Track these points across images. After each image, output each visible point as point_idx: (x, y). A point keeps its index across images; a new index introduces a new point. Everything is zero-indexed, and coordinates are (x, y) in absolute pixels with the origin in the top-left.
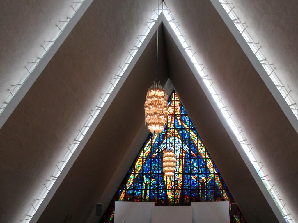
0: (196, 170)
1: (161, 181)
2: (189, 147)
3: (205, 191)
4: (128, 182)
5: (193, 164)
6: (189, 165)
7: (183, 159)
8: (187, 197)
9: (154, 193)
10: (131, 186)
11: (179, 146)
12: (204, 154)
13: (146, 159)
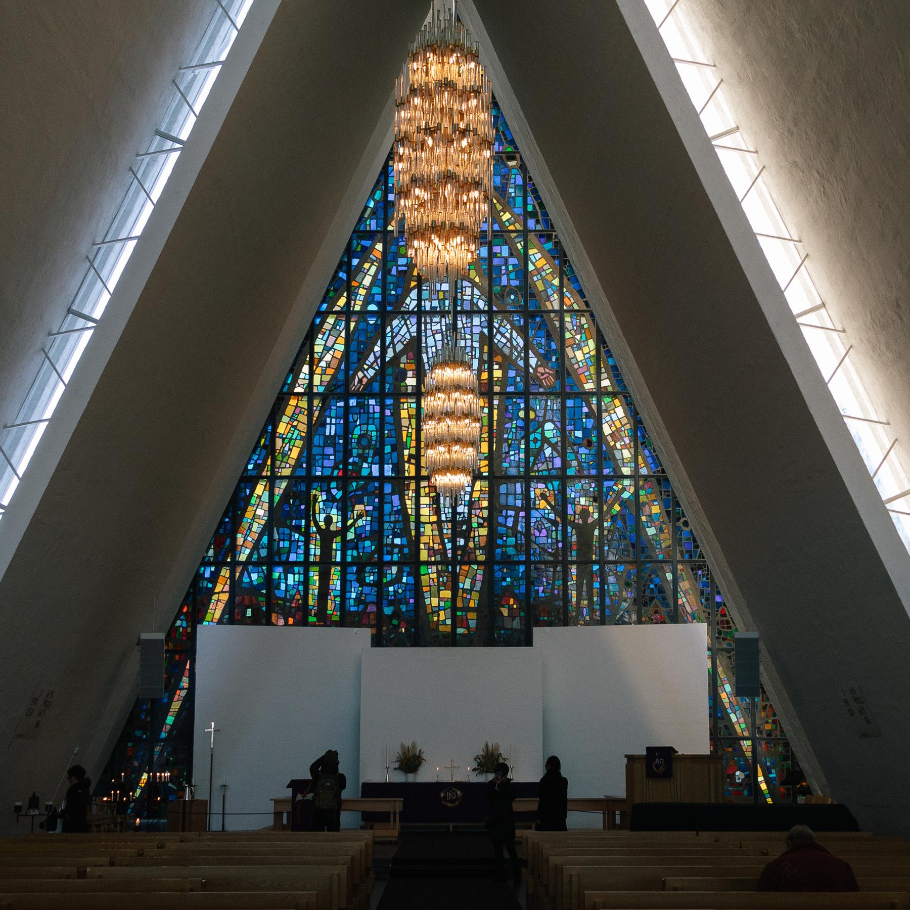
0: (552, 458)
1: (393, 519)
2: (523, 331)
3: (596, 568)
4: (245, 525)
5: (541, 425)
6: (523, 433)
7: (496, 402)
8: (512, 601)
9: (362, 582)
10: (256, 546)
11: (476, 330)
12: (592, 370)
13: (324, 397)
